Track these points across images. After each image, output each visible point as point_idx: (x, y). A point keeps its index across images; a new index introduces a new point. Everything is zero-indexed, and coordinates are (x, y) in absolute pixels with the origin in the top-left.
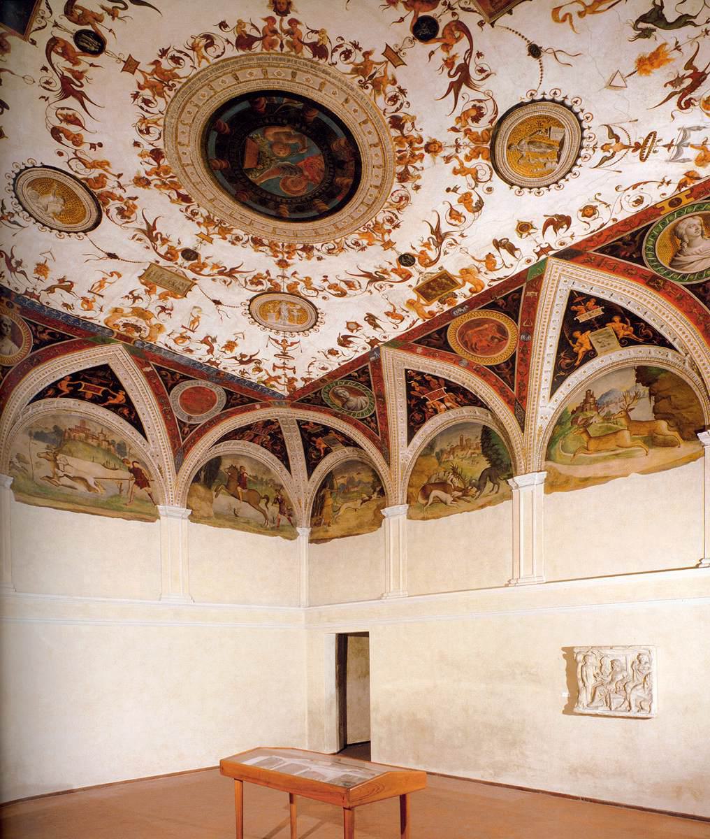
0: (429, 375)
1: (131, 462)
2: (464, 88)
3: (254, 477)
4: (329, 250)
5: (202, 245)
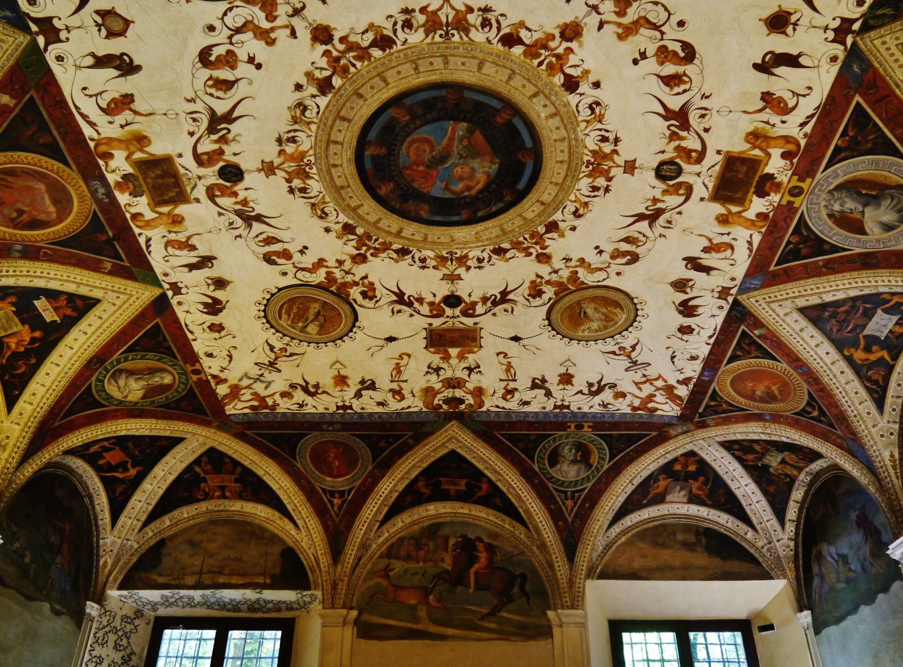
4: (305, 108)
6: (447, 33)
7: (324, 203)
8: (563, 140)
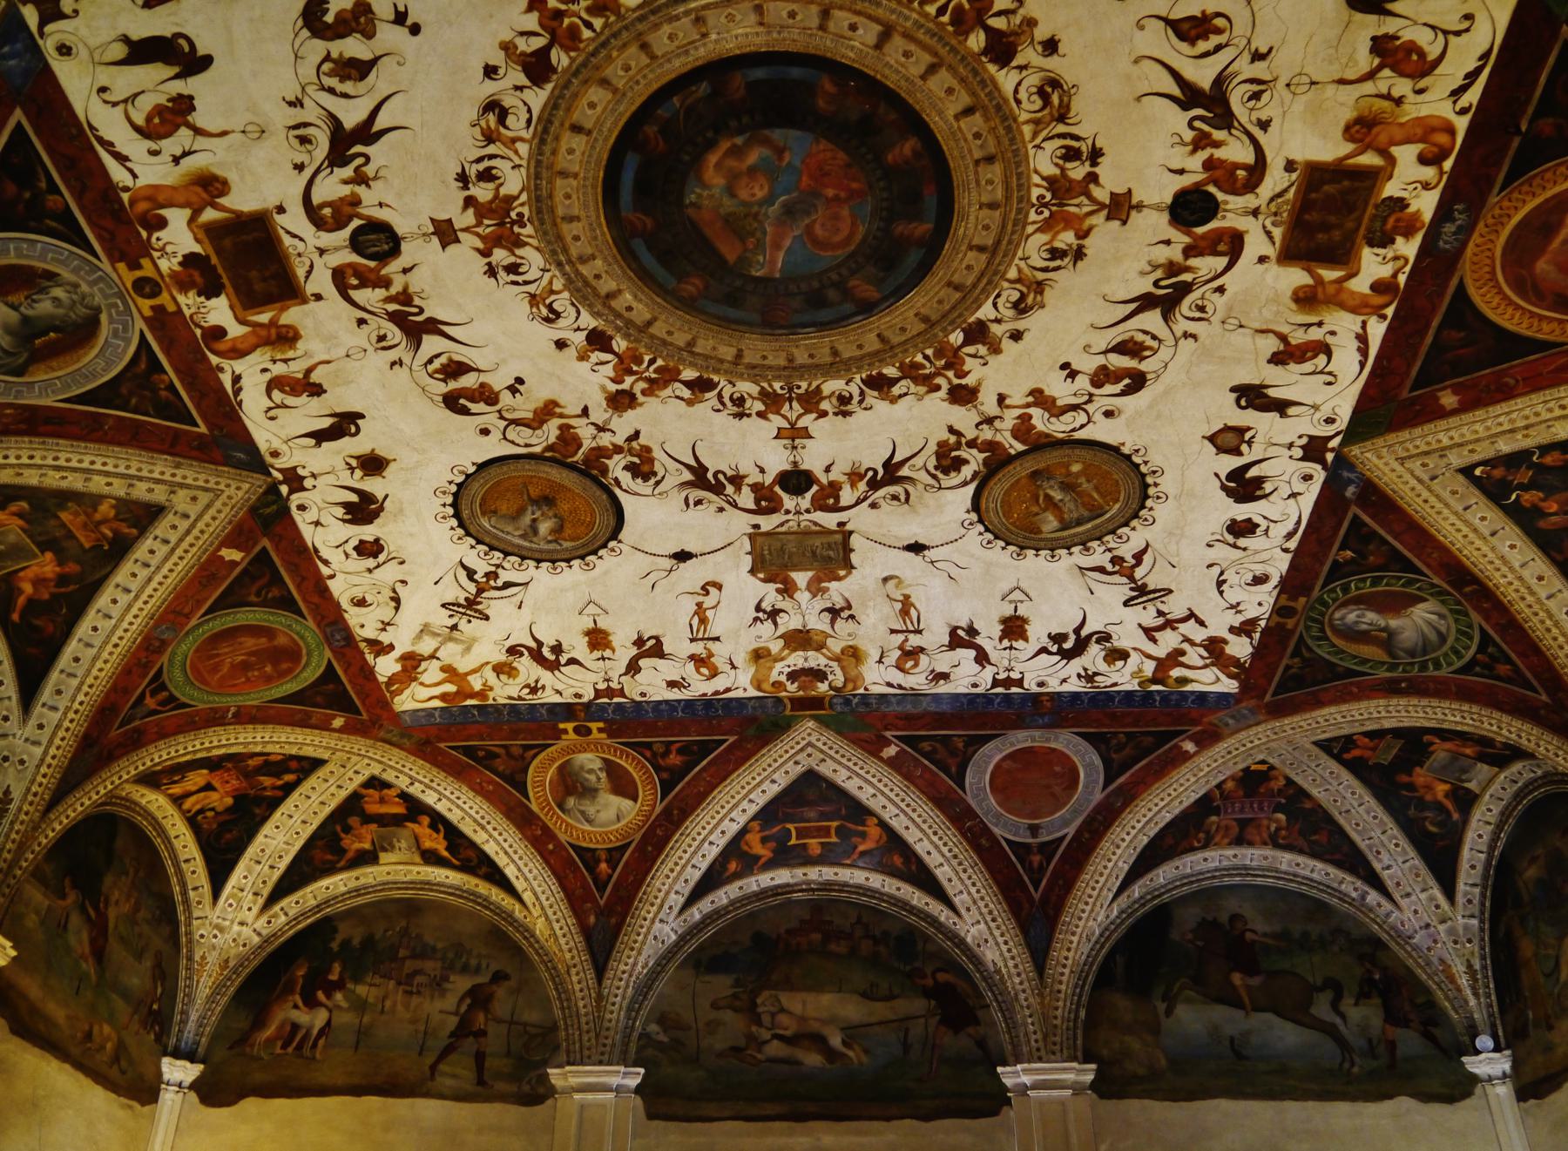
0: (1545, 449)
1: (928, 971)
3: (1274, 936)
4: (1016, 305)
6: (791, 390)
8: (583, 260)
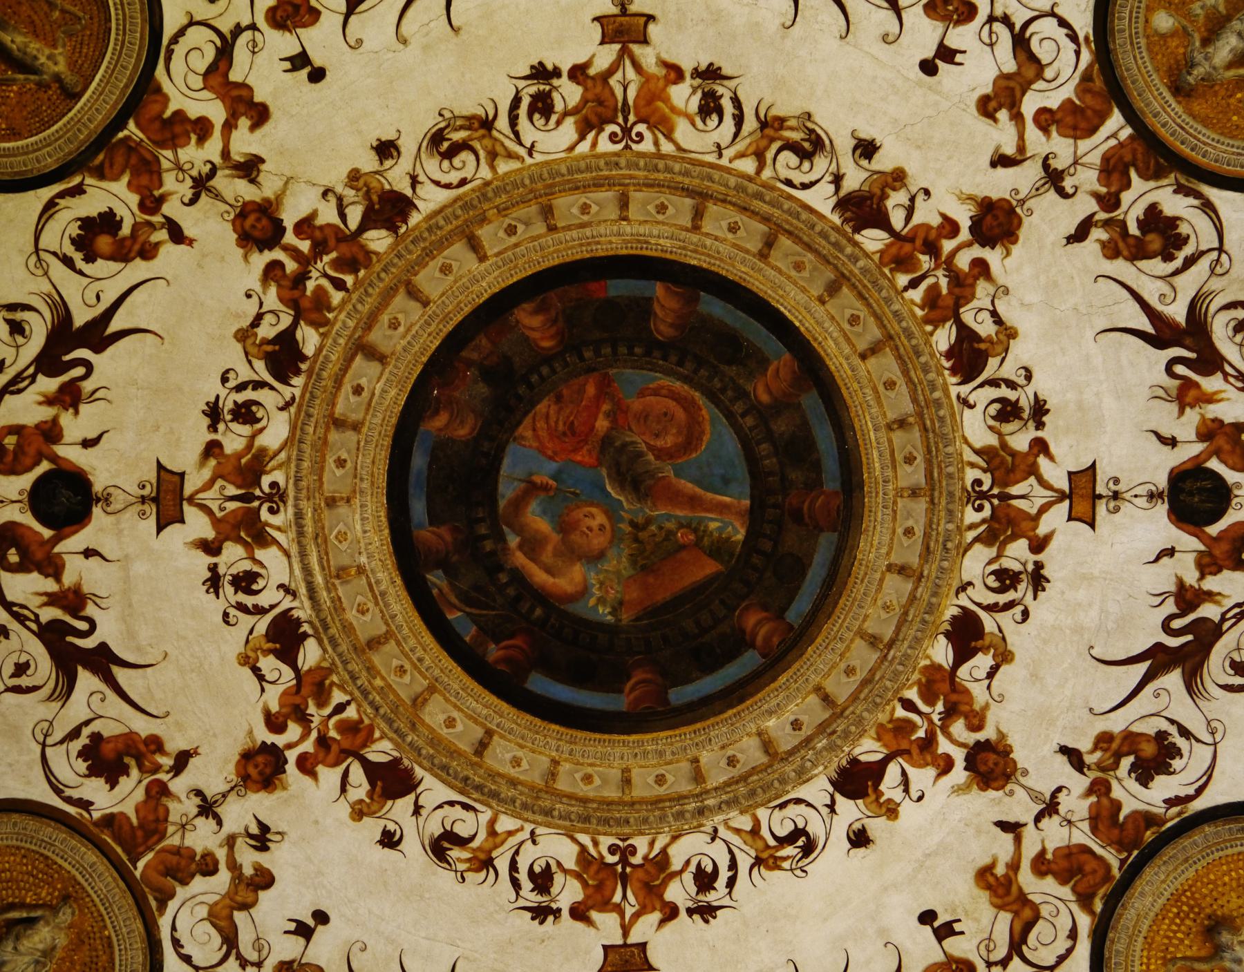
2: (81, 317)
4: (805, 155)
5: (1121, 487)
6: (983, 496)
7: (493, 156)
8: (698, 776)
